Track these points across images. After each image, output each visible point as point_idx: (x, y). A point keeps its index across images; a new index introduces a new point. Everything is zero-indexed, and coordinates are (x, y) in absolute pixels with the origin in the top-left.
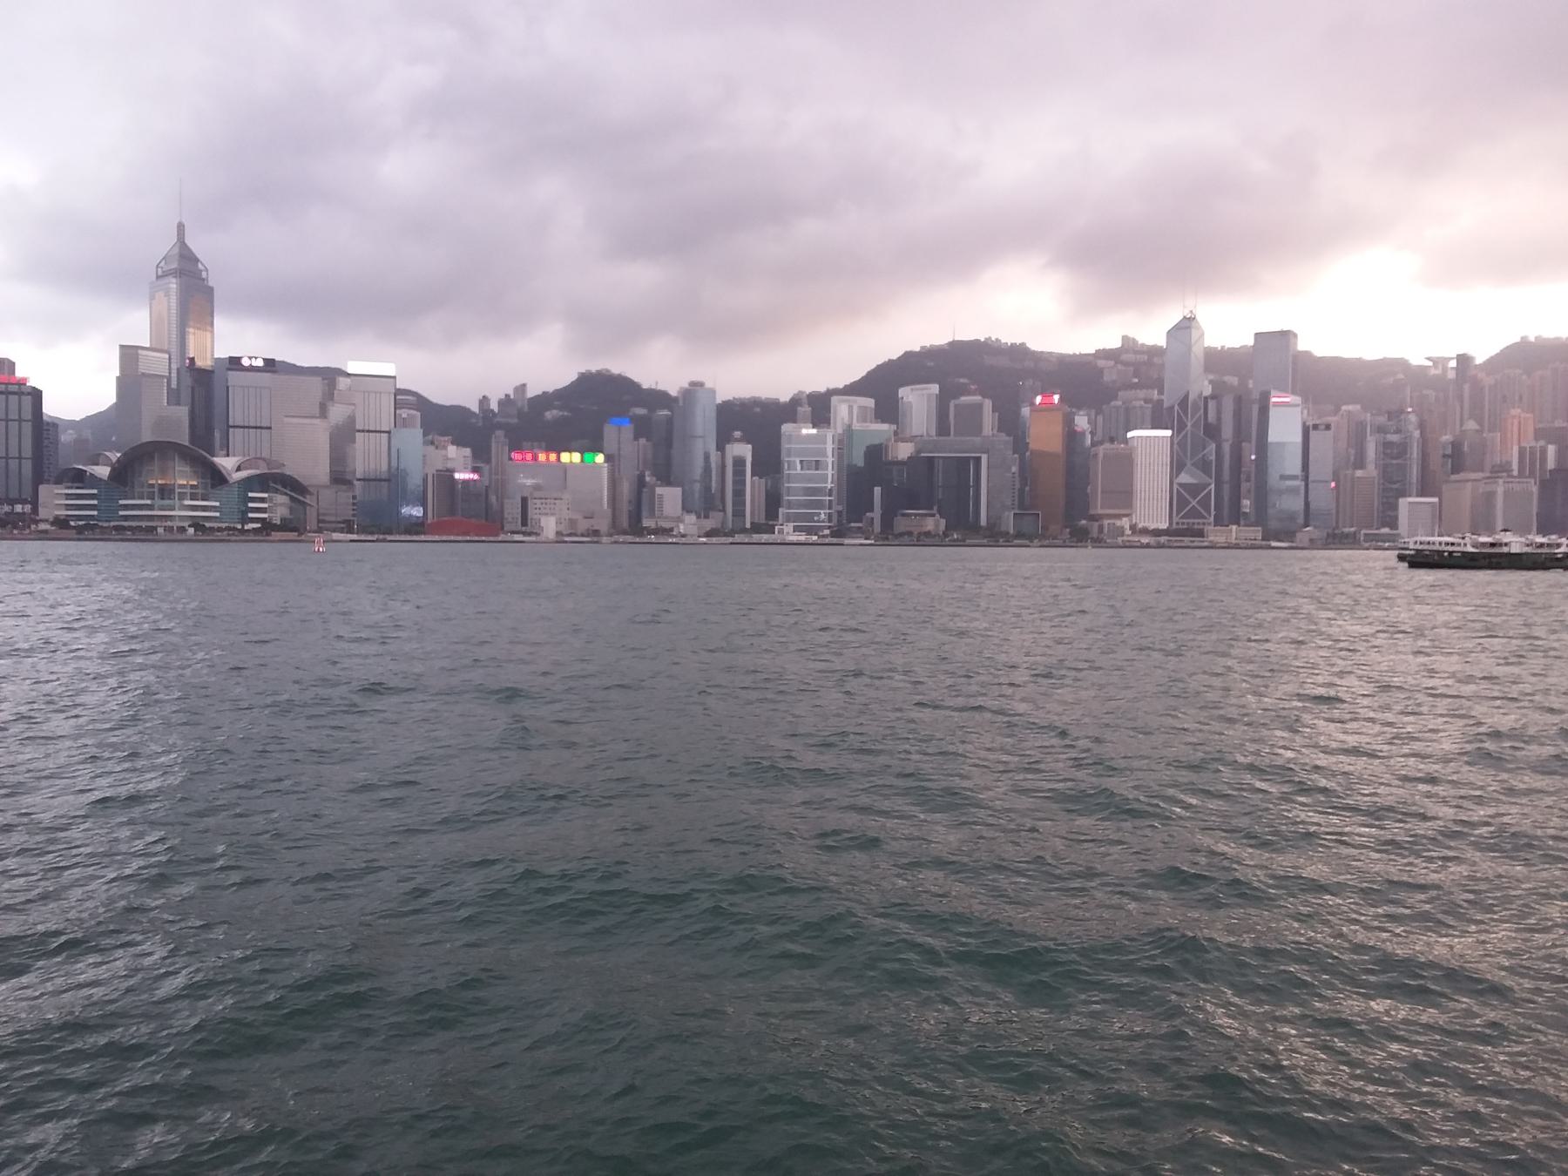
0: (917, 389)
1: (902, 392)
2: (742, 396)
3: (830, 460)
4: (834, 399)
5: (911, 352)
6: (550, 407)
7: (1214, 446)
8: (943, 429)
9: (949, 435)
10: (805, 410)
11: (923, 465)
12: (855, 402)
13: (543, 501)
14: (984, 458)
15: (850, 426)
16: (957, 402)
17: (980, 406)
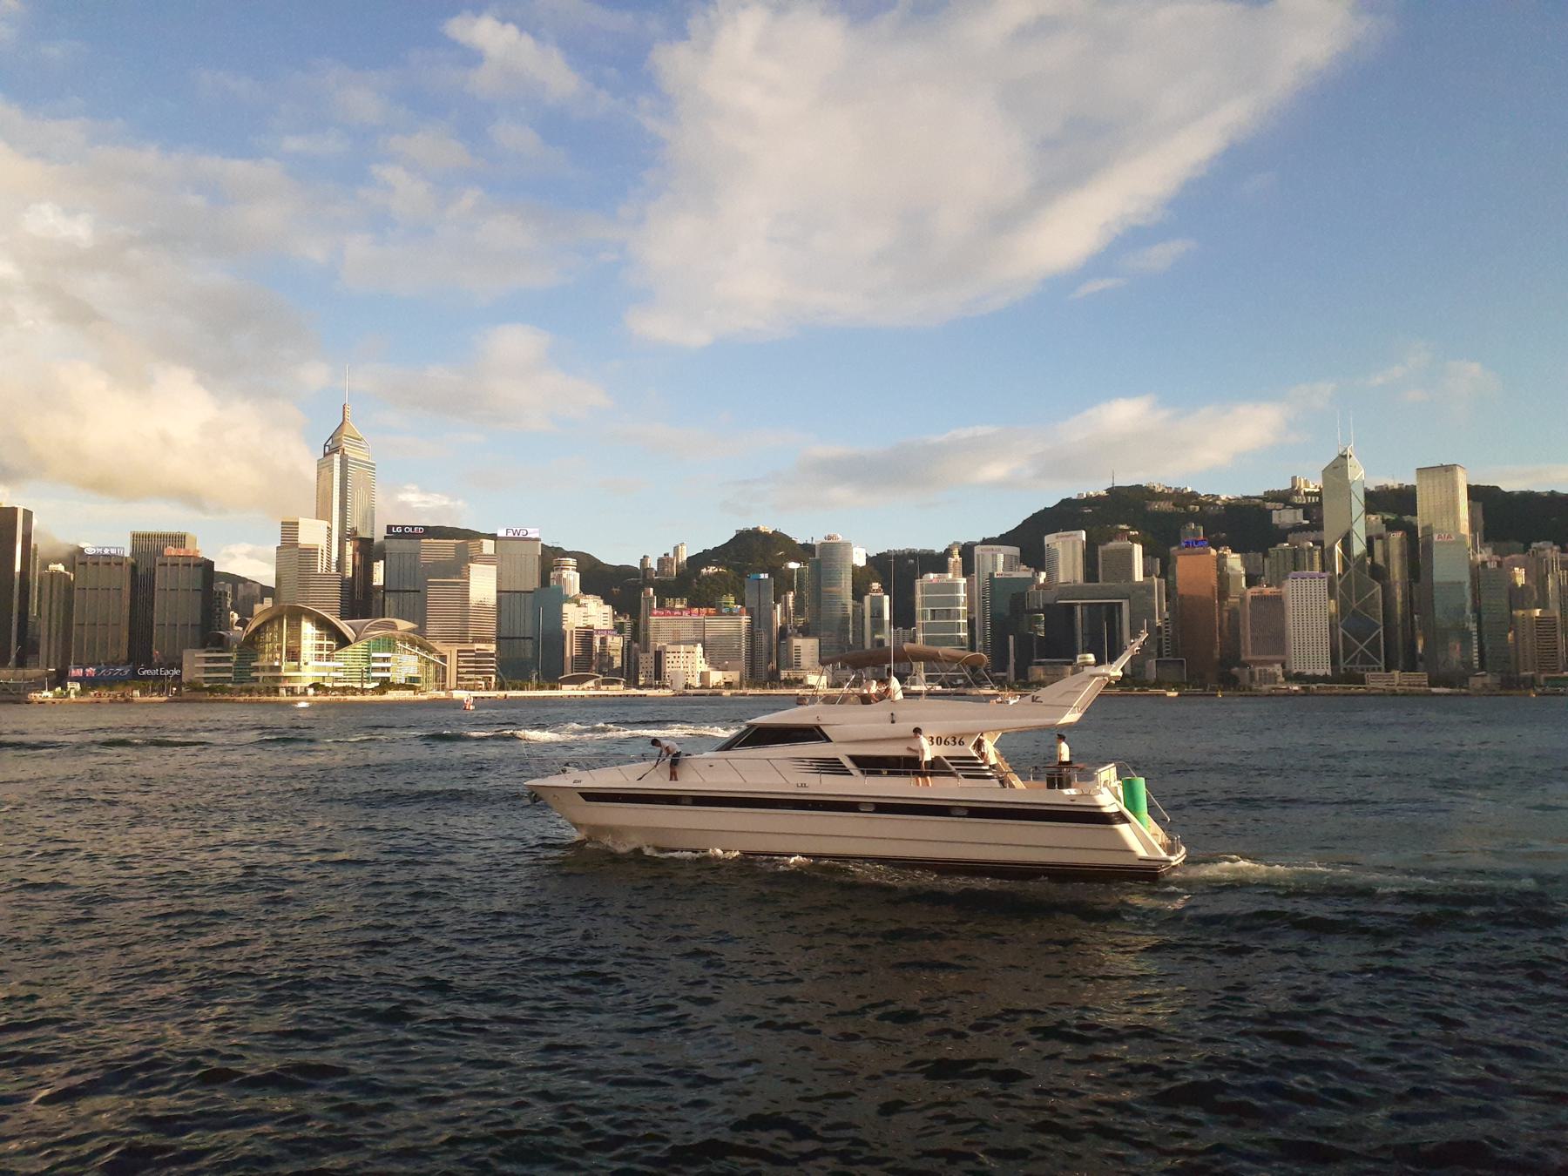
0: (1062, 536)
1: (1049, 539)
2: (897, 549)
3: (962, 608)
4: (977, 550)
5: (1069, 500)
6: (707, 564)
7: (1378, 588)
8: (1091, 573)
9: (1098, 582)
10: (955, 559)
11: (1061, 615)
12: (1000, 550)
13: (677, 655)
14: (1125, 604)
15: (991, 575)
16: (1104, 548)
17: (1130, 552)
